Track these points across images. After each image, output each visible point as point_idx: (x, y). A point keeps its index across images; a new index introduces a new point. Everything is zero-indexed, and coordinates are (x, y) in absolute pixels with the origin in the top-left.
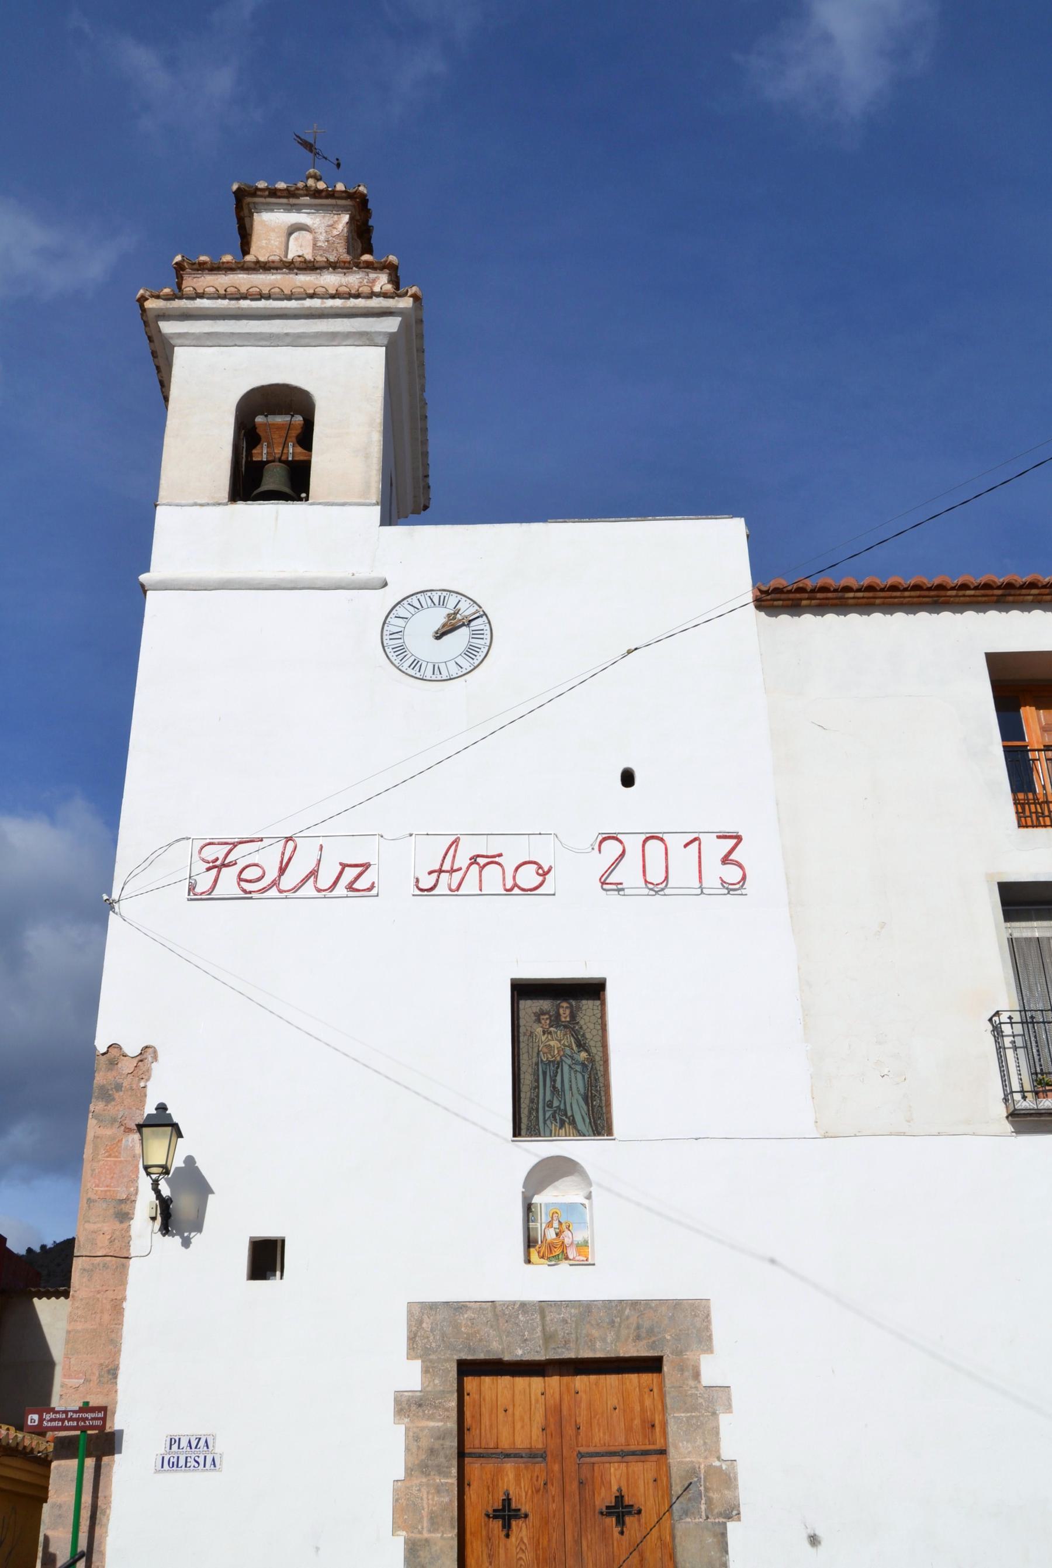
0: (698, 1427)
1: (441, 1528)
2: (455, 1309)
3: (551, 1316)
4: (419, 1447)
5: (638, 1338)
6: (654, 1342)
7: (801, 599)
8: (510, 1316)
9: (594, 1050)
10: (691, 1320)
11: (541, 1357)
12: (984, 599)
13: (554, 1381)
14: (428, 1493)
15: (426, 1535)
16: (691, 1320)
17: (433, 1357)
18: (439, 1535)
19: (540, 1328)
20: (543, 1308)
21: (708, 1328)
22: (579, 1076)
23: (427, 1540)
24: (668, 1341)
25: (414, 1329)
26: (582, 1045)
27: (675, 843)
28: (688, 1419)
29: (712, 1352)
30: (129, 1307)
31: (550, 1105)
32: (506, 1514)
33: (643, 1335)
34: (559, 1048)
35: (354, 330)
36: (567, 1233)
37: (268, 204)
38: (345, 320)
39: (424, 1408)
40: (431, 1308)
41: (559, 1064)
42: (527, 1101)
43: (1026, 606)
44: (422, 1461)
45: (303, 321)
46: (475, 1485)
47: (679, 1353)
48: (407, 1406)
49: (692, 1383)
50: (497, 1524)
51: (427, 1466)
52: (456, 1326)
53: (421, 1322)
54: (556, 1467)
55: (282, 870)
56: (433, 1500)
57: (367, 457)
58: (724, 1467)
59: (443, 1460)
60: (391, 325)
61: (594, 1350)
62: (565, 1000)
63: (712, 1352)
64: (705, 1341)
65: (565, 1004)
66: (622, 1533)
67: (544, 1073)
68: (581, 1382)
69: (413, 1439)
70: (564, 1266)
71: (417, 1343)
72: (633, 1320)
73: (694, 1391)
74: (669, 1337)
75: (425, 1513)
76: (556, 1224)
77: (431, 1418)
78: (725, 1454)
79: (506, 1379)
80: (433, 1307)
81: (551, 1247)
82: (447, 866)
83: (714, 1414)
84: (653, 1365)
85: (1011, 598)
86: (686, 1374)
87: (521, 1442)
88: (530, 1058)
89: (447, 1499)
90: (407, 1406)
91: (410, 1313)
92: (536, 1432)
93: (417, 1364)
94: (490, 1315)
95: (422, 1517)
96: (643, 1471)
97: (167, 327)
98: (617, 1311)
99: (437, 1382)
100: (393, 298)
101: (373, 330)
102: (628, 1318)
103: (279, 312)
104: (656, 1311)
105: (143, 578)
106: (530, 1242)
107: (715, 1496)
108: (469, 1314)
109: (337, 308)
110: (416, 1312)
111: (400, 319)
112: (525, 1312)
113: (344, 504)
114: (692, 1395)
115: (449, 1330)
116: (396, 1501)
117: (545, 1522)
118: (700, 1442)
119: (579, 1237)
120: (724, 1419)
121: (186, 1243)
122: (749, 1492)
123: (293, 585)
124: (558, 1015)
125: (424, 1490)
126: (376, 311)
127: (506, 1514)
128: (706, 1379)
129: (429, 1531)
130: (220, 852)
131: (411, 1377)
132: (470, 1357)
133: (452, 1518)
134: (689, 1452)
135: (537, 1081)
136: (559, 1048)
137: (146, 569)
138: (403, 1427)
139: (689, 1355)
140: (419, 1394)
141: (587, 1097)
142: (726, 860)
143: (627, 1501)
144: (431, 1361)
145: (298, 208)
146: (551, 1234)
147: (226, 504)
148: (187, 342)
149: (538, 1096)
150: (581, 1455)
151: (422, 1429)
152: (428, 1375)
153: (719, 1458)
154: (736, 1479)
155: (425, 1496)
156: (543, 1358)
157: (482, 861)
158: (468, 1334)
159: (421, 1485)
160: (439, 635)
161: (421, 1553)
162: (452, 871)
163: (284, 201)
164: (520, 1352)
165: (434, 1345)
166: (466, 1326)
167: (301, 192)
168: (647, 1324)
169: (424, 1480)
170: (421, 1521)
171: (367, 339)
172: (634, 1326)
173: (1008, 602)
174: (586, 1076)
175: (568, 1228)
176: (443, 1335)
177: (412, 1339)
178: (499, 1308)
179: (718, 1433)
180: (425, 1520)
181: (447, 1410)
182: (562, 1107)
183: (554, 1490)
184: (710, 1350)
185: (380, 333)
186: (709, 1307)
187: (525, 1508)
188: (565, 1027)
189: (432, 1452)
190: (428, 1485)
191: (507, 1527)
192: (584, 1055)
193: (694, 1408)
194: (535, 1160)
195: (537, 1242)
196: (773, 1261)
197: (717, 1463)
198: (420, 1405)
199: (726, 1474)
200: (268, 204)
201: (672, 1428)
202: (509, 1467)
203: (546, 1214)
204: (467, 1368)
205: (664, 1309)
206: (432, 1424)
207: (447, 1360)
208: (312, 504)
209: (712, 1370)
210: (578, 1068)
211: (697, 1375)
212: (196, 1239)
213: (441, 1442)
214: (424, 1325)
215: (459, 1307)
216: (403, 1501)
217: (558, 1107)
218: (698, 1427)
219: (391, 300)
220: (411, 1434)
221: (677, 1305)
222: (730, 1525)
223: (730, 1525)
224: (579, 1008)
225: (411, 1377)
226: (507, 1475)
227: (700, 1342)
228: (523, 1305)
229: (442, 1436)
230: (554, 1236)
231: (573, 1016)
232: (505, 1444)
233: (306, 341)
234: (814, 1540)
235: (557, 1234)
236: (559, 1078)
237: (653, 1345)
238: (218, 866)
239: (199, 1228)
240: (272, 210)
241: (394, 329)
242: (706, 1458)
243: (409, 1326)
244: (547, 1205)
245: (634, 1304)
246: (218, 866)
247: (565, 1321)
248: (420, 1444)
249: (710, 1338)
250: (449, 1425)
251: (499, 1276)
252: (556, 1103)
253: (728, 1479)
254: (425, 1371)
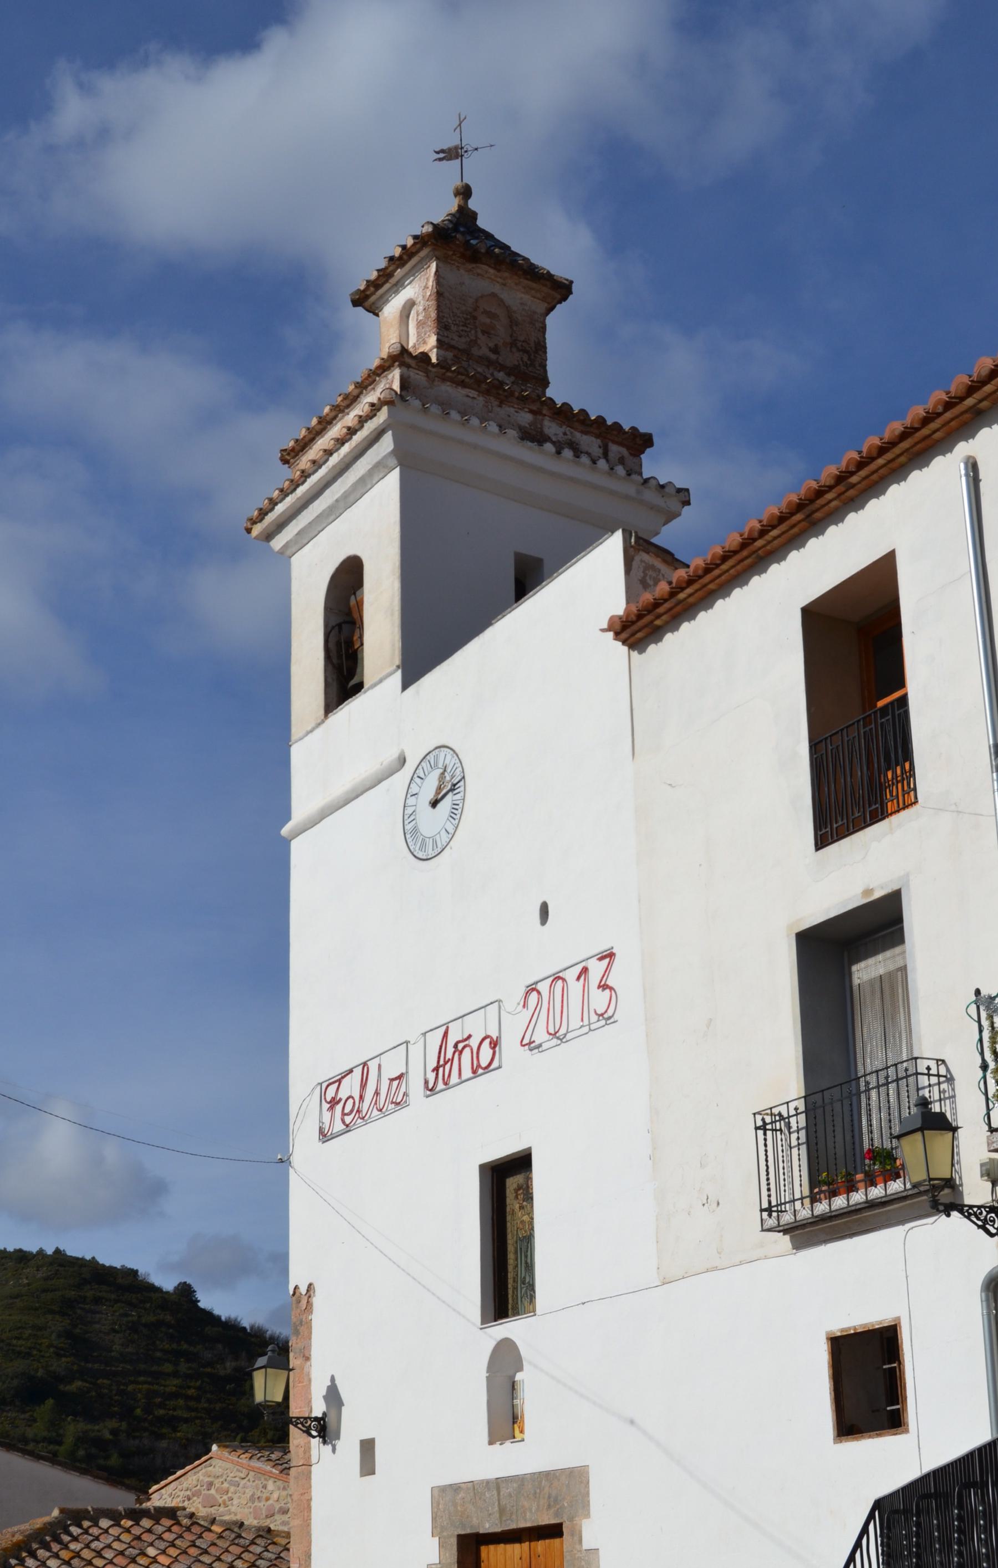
3: (504, 1491)
5: (549, 1507)
7: (652, 622)
11: (498, 1529)
12: (796, 530)
20: (498, 1484)
27: (571, 975)
30: (313, 1504)
35: (370, 467)
37: (381, 297)
38: (362, 459)
43: (836, 516)
45: (340, 480)
47: (571, 1519)
52: (455, 1505)
55: (361, 1097)
57: (392, 615)
60: (387, 443)
61: (526, 1520)
79: (501, 1546)
82: (442, 1062)
84: (554, 1531)
85: (818, 515)
88: (513, 1235)
97: (278, 543)
100: (375, 415)
101: (380, 457)
103: (324, 482)
105: (285, 831)
109: (348, 453)
111: (390, 432)
113: (381, 681)
121: (334, 1451)
123: (354, 795)
126: (372, 437)
128: (586, 1545)
130: (331, 1093)
137: (287, 817)
142: (603, 986)
145: (399, 286)
147: (323, 722)
148: (294, 550)
157: (460, 1046)
160: (434, 804)
162: (446, 1063)
163: (387, 286)
167: (391, 268)
168: (554, 1494)
171: (380, 469)
172: (547, 1496)
173: (820, 520)
184: (588, 1515)
185: (385, 457)
196: (632, 1422)
200: (381, 297)
208: (368, 689)
212: (340, 1444)
215: (455, 1488)
219: (375, 419)
228: (488, 1482)
233: (352, 499)
238: (334, 1102)
239: (338, 1438)
240: (387, 301)
241: (391, 447)
246: (334, 1102)
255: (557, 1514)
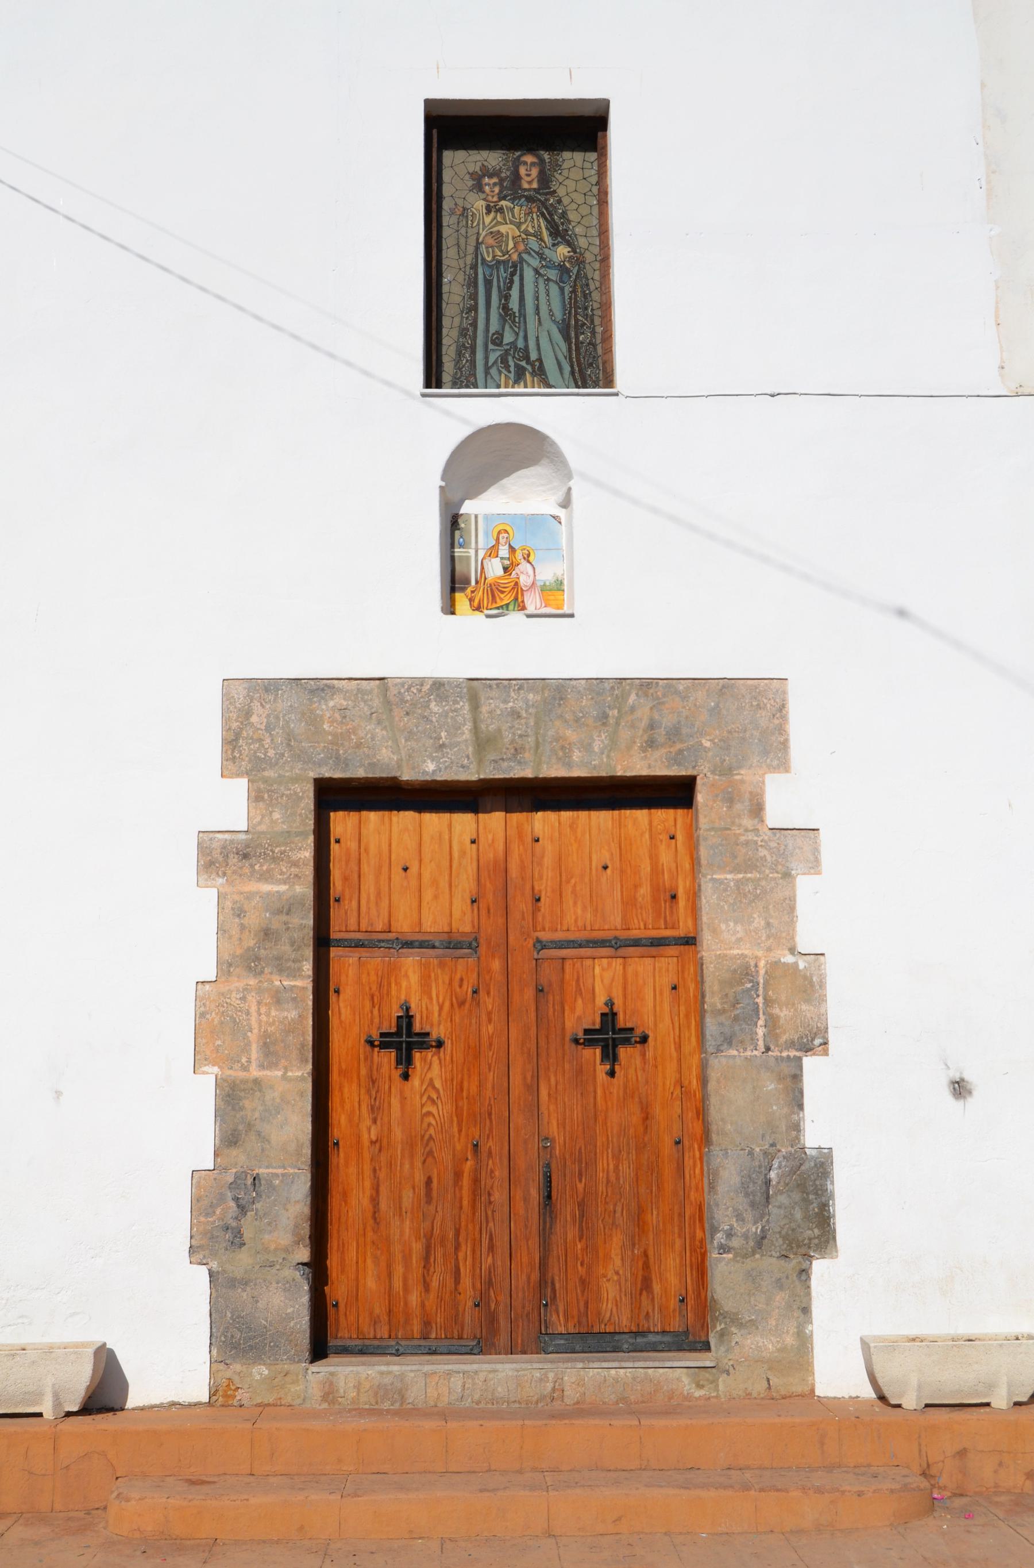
0: (757, 897)
1: (283, 1062)
2: (312, 692)
4: (243, 927)
6: (680, 752)
8: (414, 705)
9: (582, 242)
10: (752, 714)
11: (471, 774)
13: (495, 821)
14: (259, 1003)
15: (255, 1072)
16: (752, 714)
17: (270, 773)
18: (279, 1073)
19: (468, 727)
20: (475, 689)
21: (781, 729)
22: (554, 289)
23: (257, 1082)
24: (706, 750)
25: (235, 725)
26: (559, 233)
28: (738, 882)
29: (787, 770)
31: (497, 340)
32: (404, 1041)
33: (661, 739)
34: (514, 208)
36: (524, 566)
39: (253, 860)
40: (267, 690)
41: (516, 268)
42: (455, 333)
44: (249, 949)
46: (348, 992)
47: (728, 771)
48: (222, 857)
49: (748, 822)
50: (387, 1058)
51: (258, 959)
52: (314, 721)
53: (248, 714)
54: (496, 965)
56: (268, 1015)
58: (802, 965)
59: (287, 948)
61: (569, 765)
62: (531, 150)
63: (787, 770)
64: (776, 750)
65: (529, 159)
66: (612, 1074)
67: (488, 283)
68: (543, 822)
69: (232, 913)
70: (515, 619)
71: (238, 750)
72: (644, 713)
73: (751, 836)
74: (707, 744)
75: (253, 1036)
76: (504, 551)
77: (266, 877)
78: (805, 942)
79: (408, 817)
80: (270, 687)
81: (494, 590)
83: (787, 875)
84: (677, 793)
86: (738, 807)
87: (433, 923)
88: (461, 254)
89: (293, 1014)
90: (222, 857)
91: (227, 698)
92: (460, 905)
93: (241, 785)
94: (376, 703)
95: (249, 1044)
96: (653, 973)
98: (610, 698)
99: (276, 816)
102: (633, 709)
104: (685, 698)
106: (454, 583)
107: (783, 1014)
108: (338, 701)
110: (239, 693)
112: (442, 698)
114: (747, 843)
115: (299, 728)
116: (201, 1016)
117: (474, 1053)
118: (758, 922)
119: (546, 574)
120: (805, 886)
122: (846, 1007)
124: (516, 178)
125: (252, 999)
127: (404, 1041)
128: (775, 815)
129: (262, 1067)
131: (230, 806)
132: (338, 775)
133: (303, 1046)
134: (740, 940)
135: (474, 297)
136: (514, 208)
138: (212, 894)
139: (744, 774)
140: (243, 837)
141: (568, 326)
143: (622, 1022)
144: (266, 780)
146: (495, 569)
149: (474, 325)
150: (541, 945)
151: (250, 896)
152: (261, 804)
153: (792, 950)
154: (822, 984)
155: (253, 1009)
156: (474, 778)
158: (335, 735)
159: (246, 989)
161: (246, 1103)
164: (431, 767)
165: (271, 753)
166: (332, 722)
168: (667, 720)
169: (253, 982)
170: (246, 1048)
172: (644, 724)
174: (567, 289)
175: (527, 558)
176: (289, 736)
177: (231, 742)
178: (393, 691)
179: (792, 909)
180: (254, 1047)
181: (295, 864)
182: (520, 344)
183: (490, 1002)
184: (783, 765)
186: (785, 692)
187: (437, 1032)
188: (530, 199)
189: (267, 934)
190: (260, 991)
191: (405, 1062)
192: (563, 251)
193: (750, 865)
194: (466, 431)
195: (468, 582)
197: (789, 959)
198: (246, 856)
199: (805, 978)
201: (709, 898)
202: (411, 962)
203: (486, 534)
204: (334, 796)
205: (700, 695)
206: (266, 888)
207: (295, 780)
209: (784, 802)
210: (553, 274)
211: (758, 810)
213: (284, 918)
214: (254, 719)
215: (319, 688)
216: (214, 1017)
217: (513, 344)
218: (757, 897)
220: (228, 904)
221: (725, 687)
222: (809, 1063)
223: (809, 1063)
224: (557, 166)
225: (230, 806)
226: (406, 976)
227: (766, 752)
228: (439, 686)
229: (286, 908)
230: (501, 572)
231: (544, 180)
232: (403, 925)
234: (960, 1088)
235: (506, 569)
236: (515, 293)
237: (677, 758)
242: (769, 949)
243: (226, 720)
244: (486, 517)
245: (646, 685)
247: (515, 714)
248: (245, 921)
249: (785, 745)
250: (298, 889)
251: (387, 630)
252: (508, 337)
253: (808, 986)
254: (256, 797)
255: (677, 758)
